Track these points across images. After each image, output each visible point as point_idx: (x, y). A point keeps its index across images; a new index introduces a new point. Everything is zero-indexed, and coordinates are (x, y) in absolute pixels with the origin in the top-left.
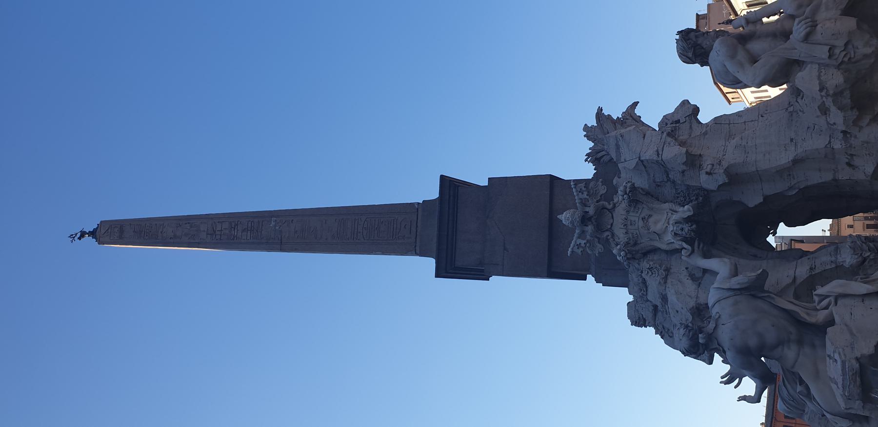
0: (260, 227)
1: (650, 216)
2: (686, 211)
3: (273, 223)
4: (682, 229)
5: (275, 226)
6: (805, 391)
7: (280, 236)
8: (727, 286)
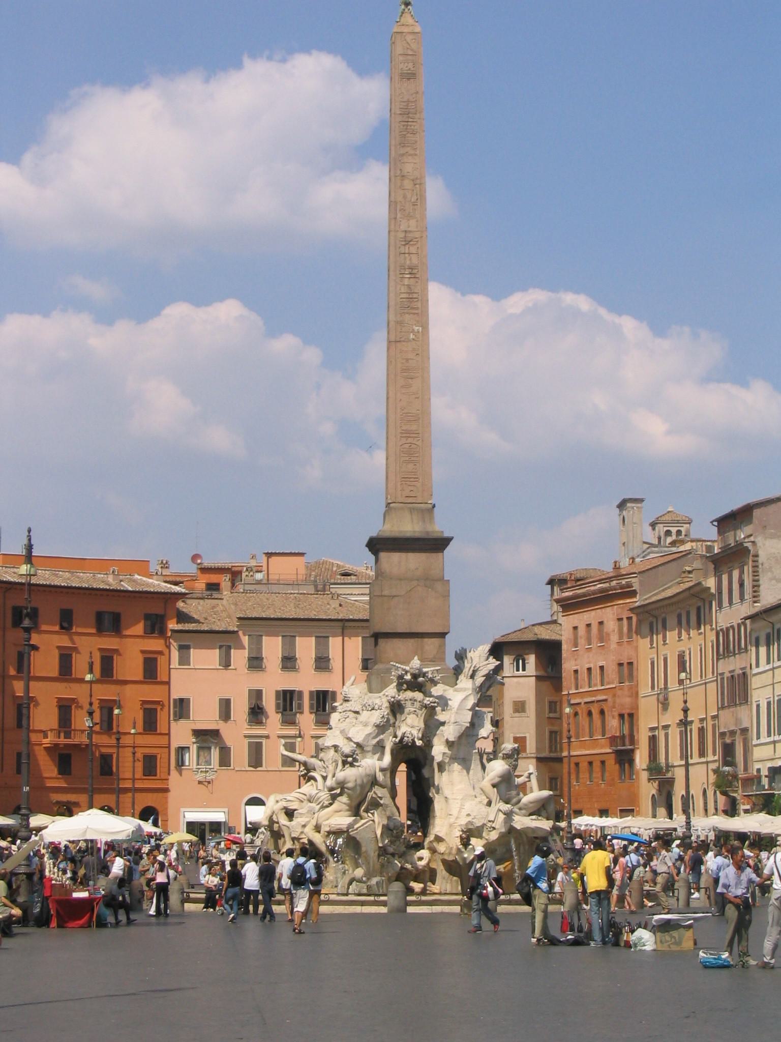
1: (417, 716)
2: (419, 743)
3: (416, 328)
4: (408, 737)
5: (413, 331)
6: (324, 805)
8: (377, 770)
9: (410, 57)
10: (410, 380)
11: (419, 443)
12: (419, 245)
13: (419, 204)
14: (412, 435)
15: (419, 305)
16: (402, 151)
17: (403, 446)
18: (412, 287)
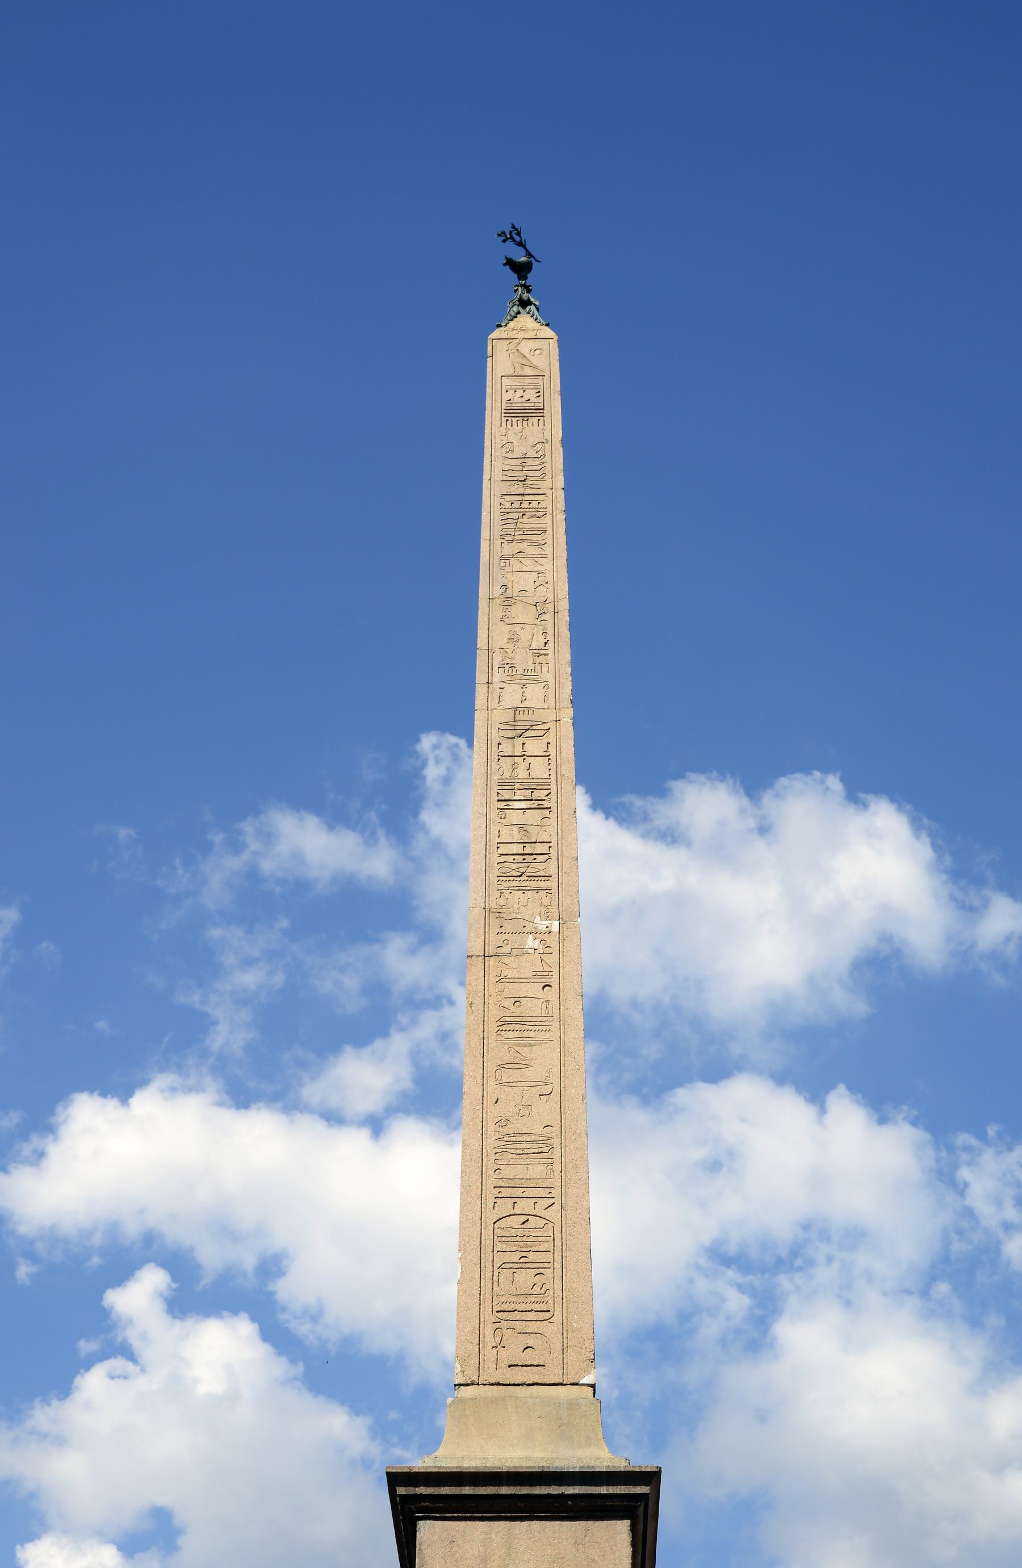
0: (533, 884)
3: (542, 924)
7: (506, 950)
9: (527, 380)
10: (524, 1051)
11: (549, 1214)
12: (551, 737)
13: (551, 652)
14: (529, 1193)
15: (552, 868)
16: (508, 549)
17: (503, 1223)
18: (530, 829)
